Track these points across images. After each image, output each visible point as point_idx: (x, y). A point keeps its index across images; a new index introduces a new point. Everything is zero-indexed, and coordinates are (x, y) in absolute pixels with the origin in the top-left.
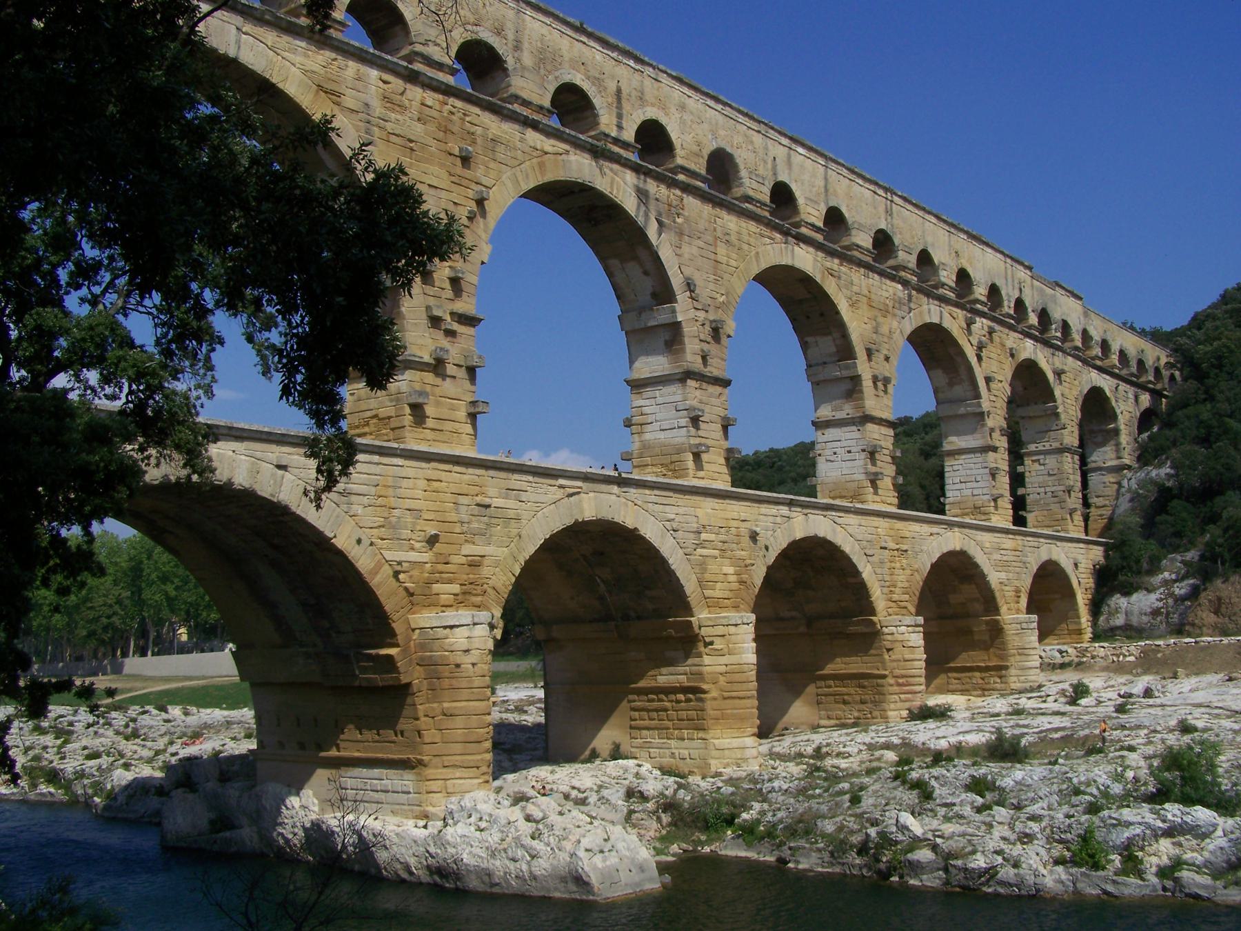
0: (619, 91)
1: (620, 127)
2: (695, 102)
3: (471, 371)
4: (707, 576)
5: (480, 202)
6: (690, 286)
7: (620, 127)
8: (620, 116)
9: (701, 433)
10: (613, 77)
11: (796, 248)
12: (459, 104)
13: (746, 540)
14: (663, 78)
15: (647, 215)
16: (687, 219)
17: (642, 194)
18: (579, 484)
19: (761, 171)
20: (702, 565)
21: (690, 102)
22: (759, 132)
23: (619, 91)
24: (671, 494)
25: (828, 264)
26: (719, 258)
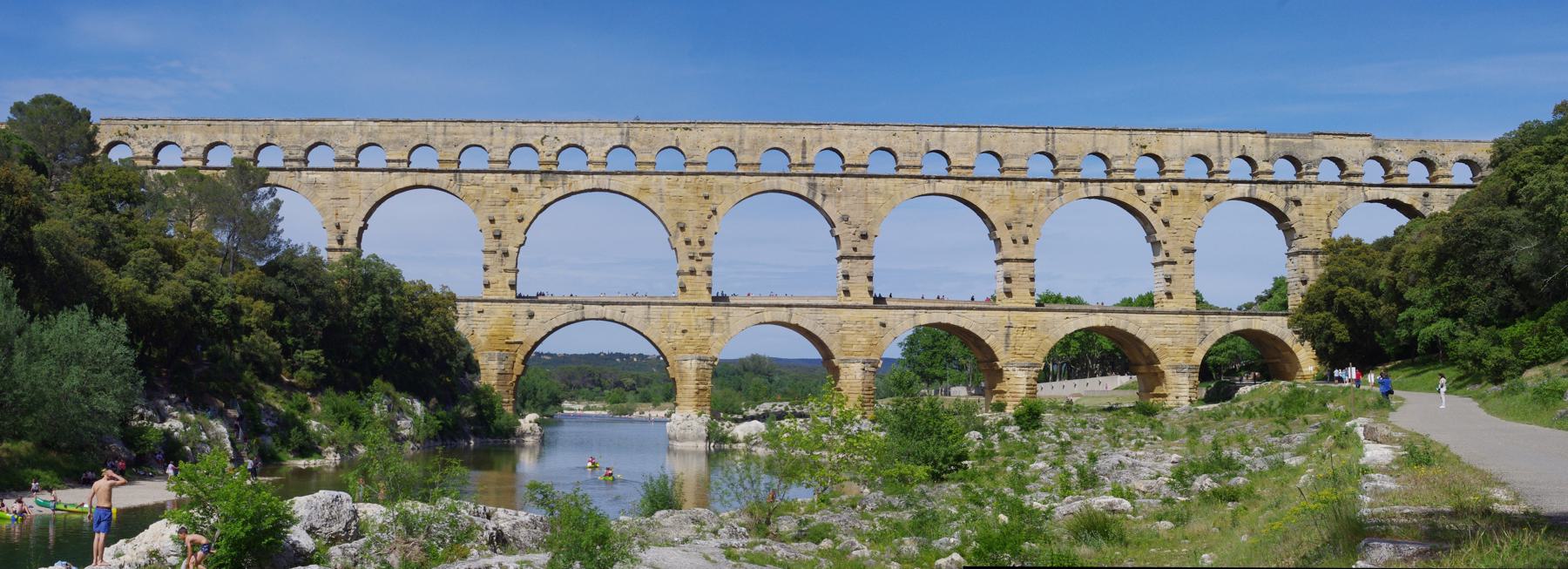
0: (804, 143)
2: (860, 131)
3: (710, 273)
6: (845, 219)
13: (878, 327)
17: (813, 186)
19: (915, 149)
20: (843, 338)
23: (804, 143)
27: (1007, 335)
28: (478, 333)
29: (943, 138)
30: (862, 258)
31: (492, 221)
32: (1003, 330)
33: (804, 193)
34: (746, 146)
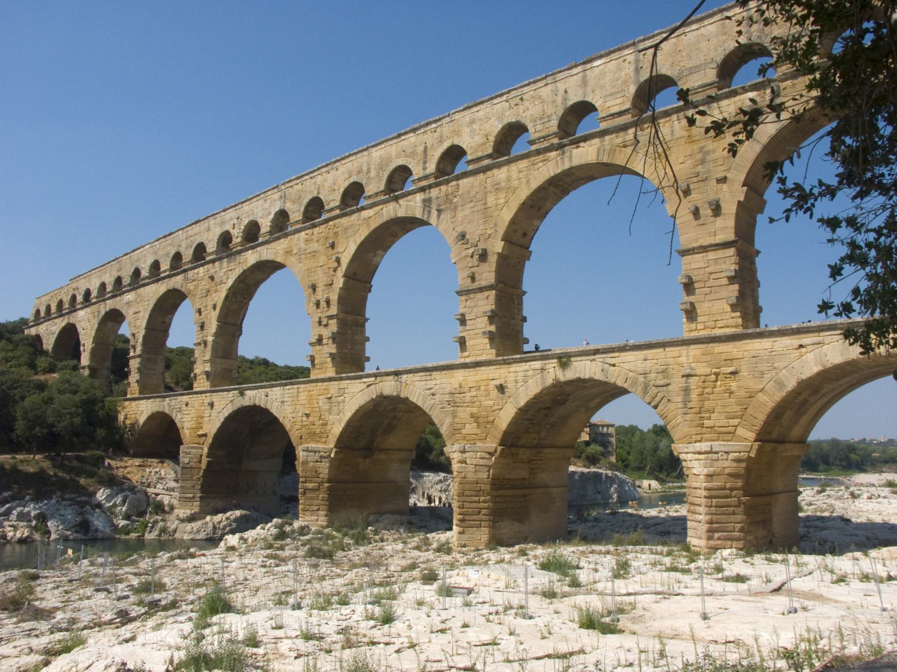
0: (426, 148)
1: (425, 169)
4: (457, 420)
5: (338, 260)
7: (425, 169)
8: (425, 163)
9: (467, 328)
10: (421, 144)
11: (575, 151)
12: (331, 223)
13: (495, 393)
14: (457, 116)
15: (429, 212)
16: (462, 196)
18: (373, 379)
19: (550, 110)
21: (481, 113)
22: (547, 85)
24: (617, 354)
25: (619, 140)
26: (489, 205)
27: (686, 391)
28: (186, 425)
29: (584, 82)
30: (481, 289)
31: (200, 312)
32: (677, 383)
33: (418, 215)
34: (373, 174)
